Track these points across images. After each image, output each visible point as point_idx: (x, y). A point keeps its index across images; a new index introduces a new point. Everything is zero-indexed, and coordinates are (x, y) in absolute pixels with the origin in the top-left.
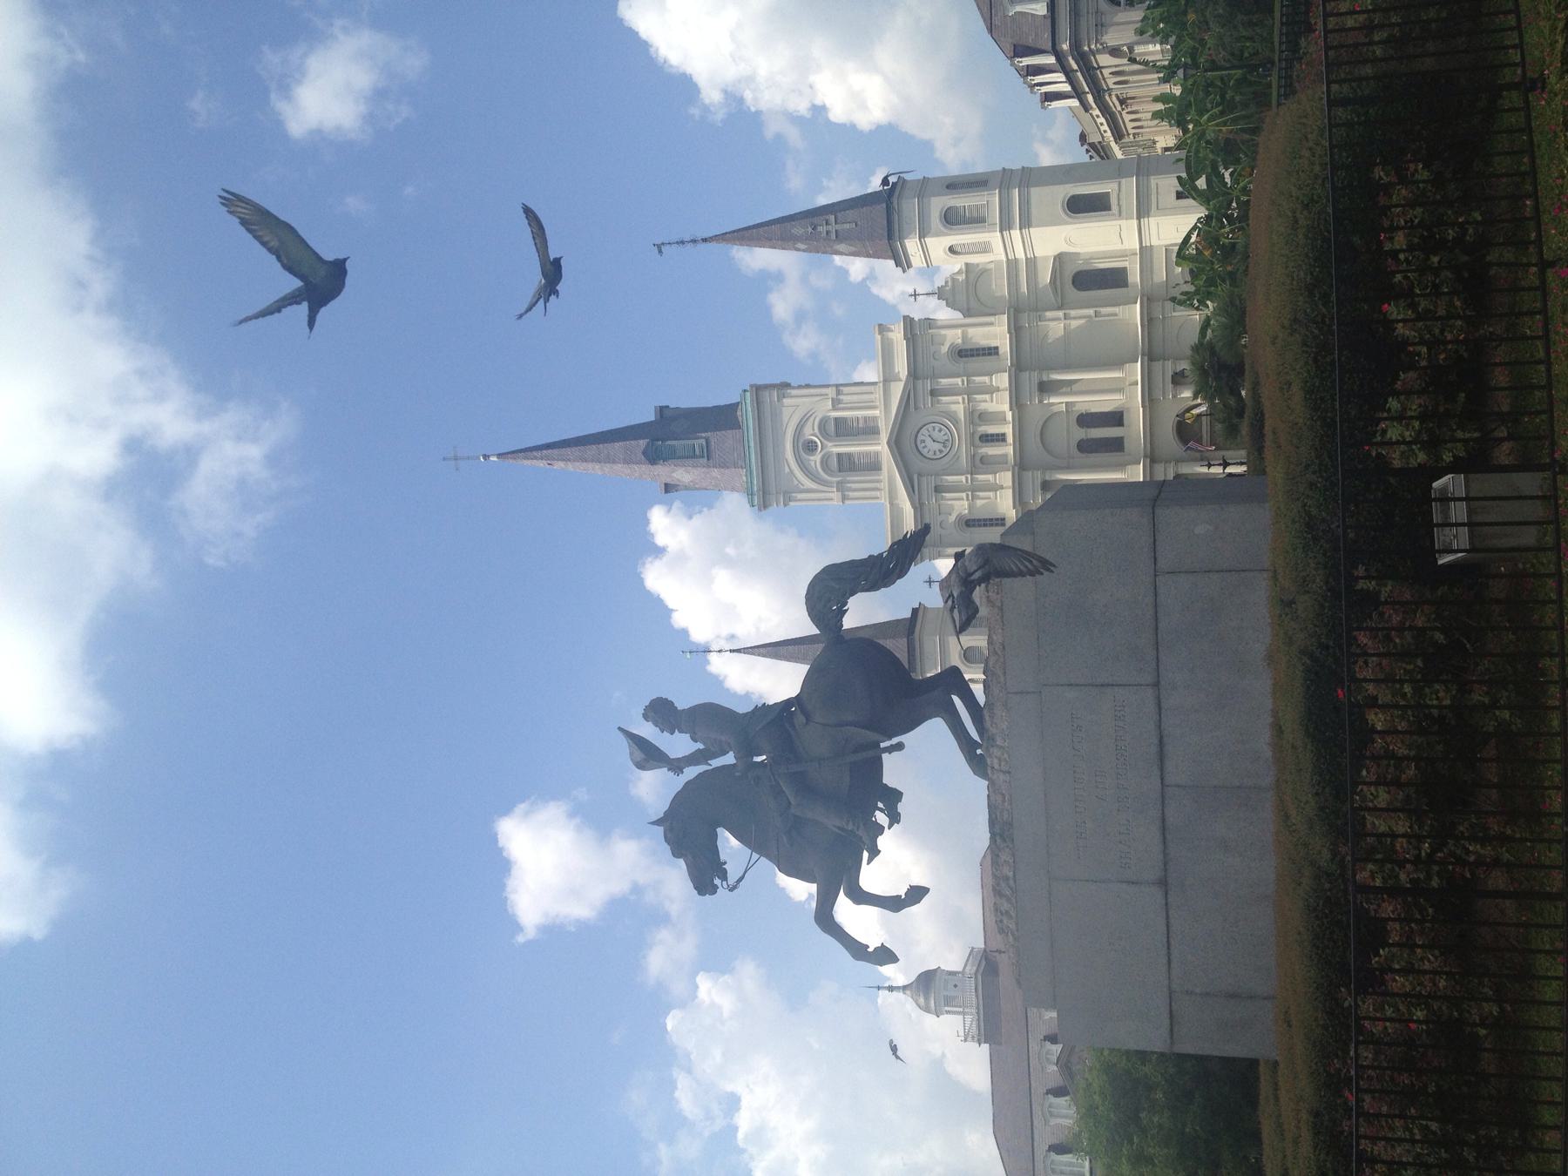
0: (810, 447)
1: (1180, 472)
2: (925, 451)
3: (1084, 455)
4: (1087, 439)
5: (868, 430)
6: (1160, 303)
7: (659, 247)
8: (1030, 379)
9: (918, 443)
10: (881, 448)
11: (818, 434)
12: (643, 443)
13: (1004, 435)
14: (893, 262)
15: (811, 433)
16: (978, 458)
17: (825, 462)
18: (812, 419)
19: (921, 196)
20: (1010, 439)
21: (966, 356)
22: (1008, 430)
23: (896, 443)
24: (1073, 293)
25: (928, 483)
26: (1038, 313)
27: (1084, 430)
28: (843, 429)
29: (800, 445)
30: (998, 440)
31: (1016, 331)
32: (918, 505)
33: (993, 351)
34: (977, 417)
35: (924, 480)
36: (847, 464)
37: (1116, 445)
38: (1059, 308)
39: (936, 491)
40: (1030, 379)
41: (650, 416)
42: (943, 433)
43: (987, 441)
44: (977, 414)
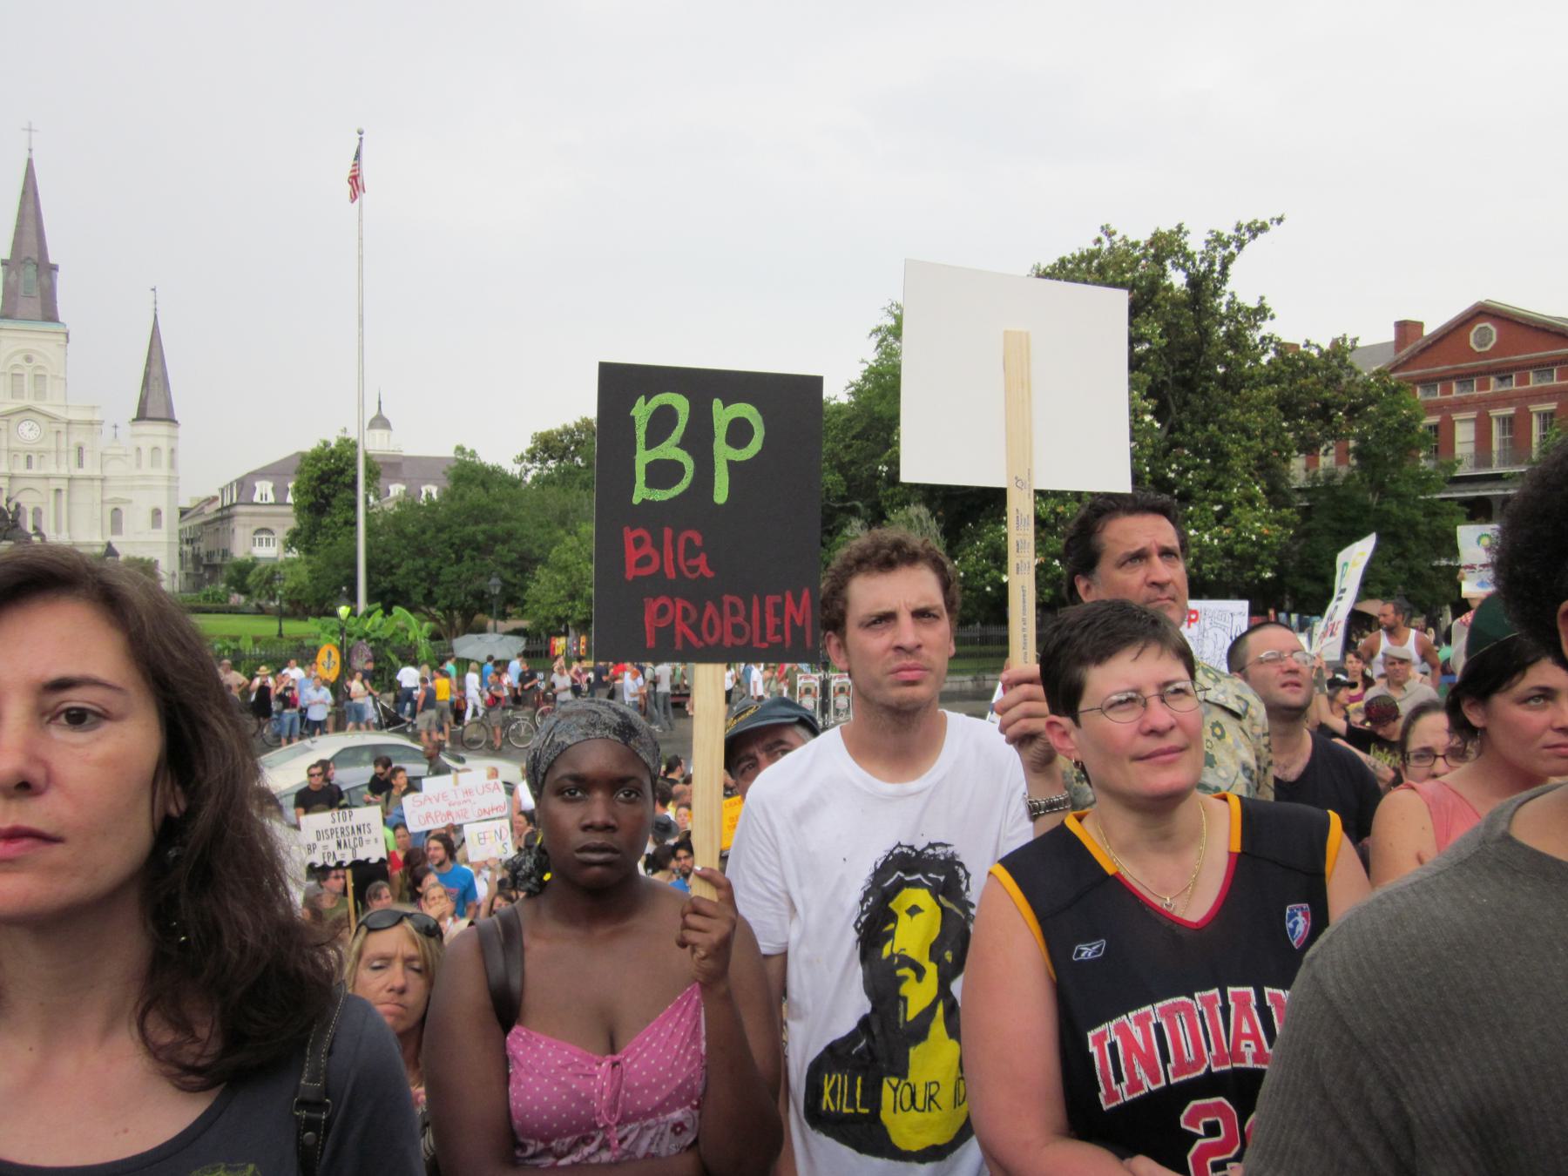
0: (29, 359)
2: (23, 424)
5: (40, 394)
7: (154, 290)
8: (63, 485)
10: (26, 402)
12: (35, 256)
15: (38, 360)
17: (16, 366)
19: (169, 437)
20: (29, 472)
22: (34, 471)
23: (29, 410)
24: (109, 507)
28: (39, 378)
31: (91, 479)
33: (80, 465)
34: (42, 454)
35: (5, 423)
40: (63, 485)
41: (52, 260)
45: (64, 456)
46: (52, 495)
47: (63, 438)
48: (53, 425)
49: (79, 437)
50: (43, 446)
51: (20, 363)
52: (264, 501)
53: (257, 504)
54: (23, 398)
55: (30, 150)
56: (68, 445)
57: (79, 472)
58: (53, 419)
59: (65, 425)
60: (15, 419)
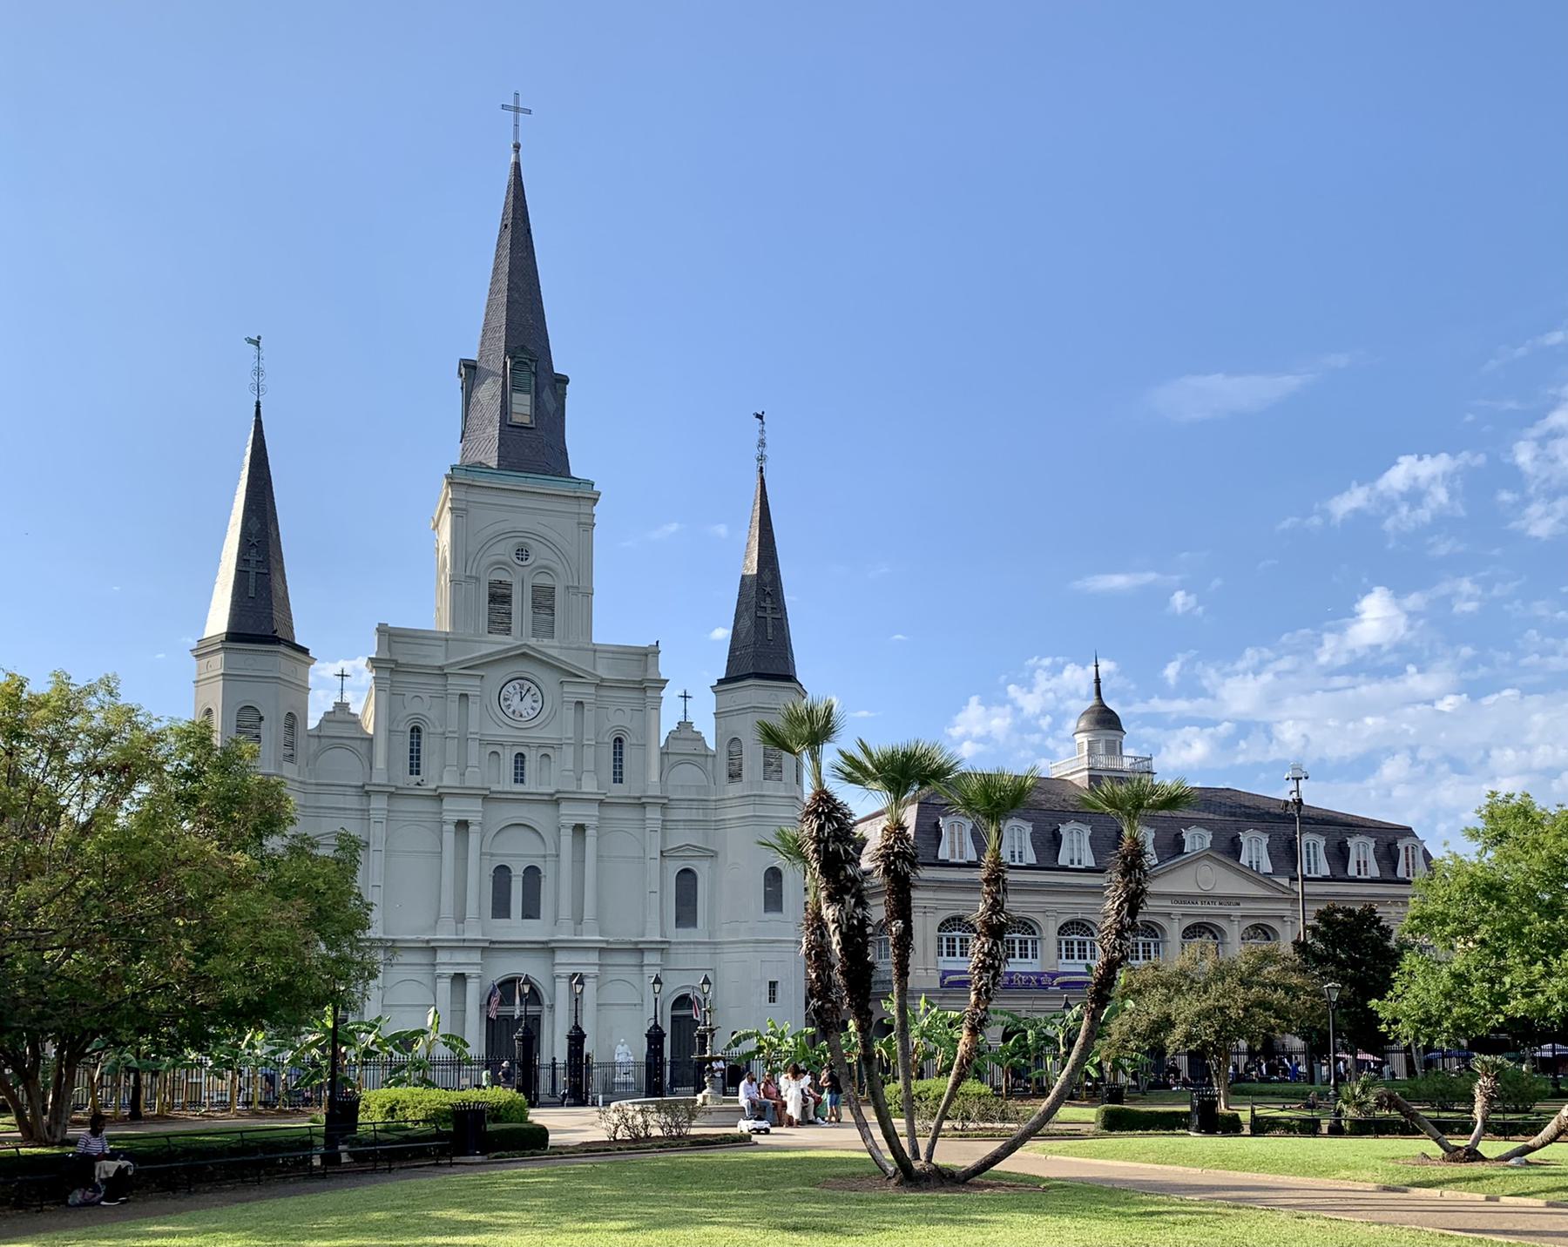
0: (522, 553)
1: (469, 980)
2: (509, 687)
3: (492, 873)
4: (510, 878)
6: (659, 962)
8: (587, 814)
9: (519, 681)
11: (534, 566)
13: (522, 781)
14: (723, 677)
15: (540, 555)
16: (498, 749)
17: (500, 565)
18: (556, 559)
20: (519, 788)
21: (615, 747)
22: (530, 786)
23: (524, 654)
24: (675, 867)
25: (471, 686)
26: (659, 830)
27: (521, 873)
29: (526, 540)
30: (516, 774)
32: (445, 671)
33: (618, 778)
35: (477, 682)
36: (499, 597)
37: (501, 908)
38: (662, 852)
39: (461, 695)
42: (530, 711)
43: (516, 762)
44: (549, 751)
45: (589, 753)
46: (567, 838)
47: (589, 714)
48: (567, 688)
49: (618, 714)
50: (548, 734)
51: (509, 559)
52: (957, 860)
53: (945, 864)
54: (508, 631)
55: (517, 147)
56: (597, 735)
57: (618, 790)
58: (569, 675)
59: (592, 690)
60: (498, 675)
